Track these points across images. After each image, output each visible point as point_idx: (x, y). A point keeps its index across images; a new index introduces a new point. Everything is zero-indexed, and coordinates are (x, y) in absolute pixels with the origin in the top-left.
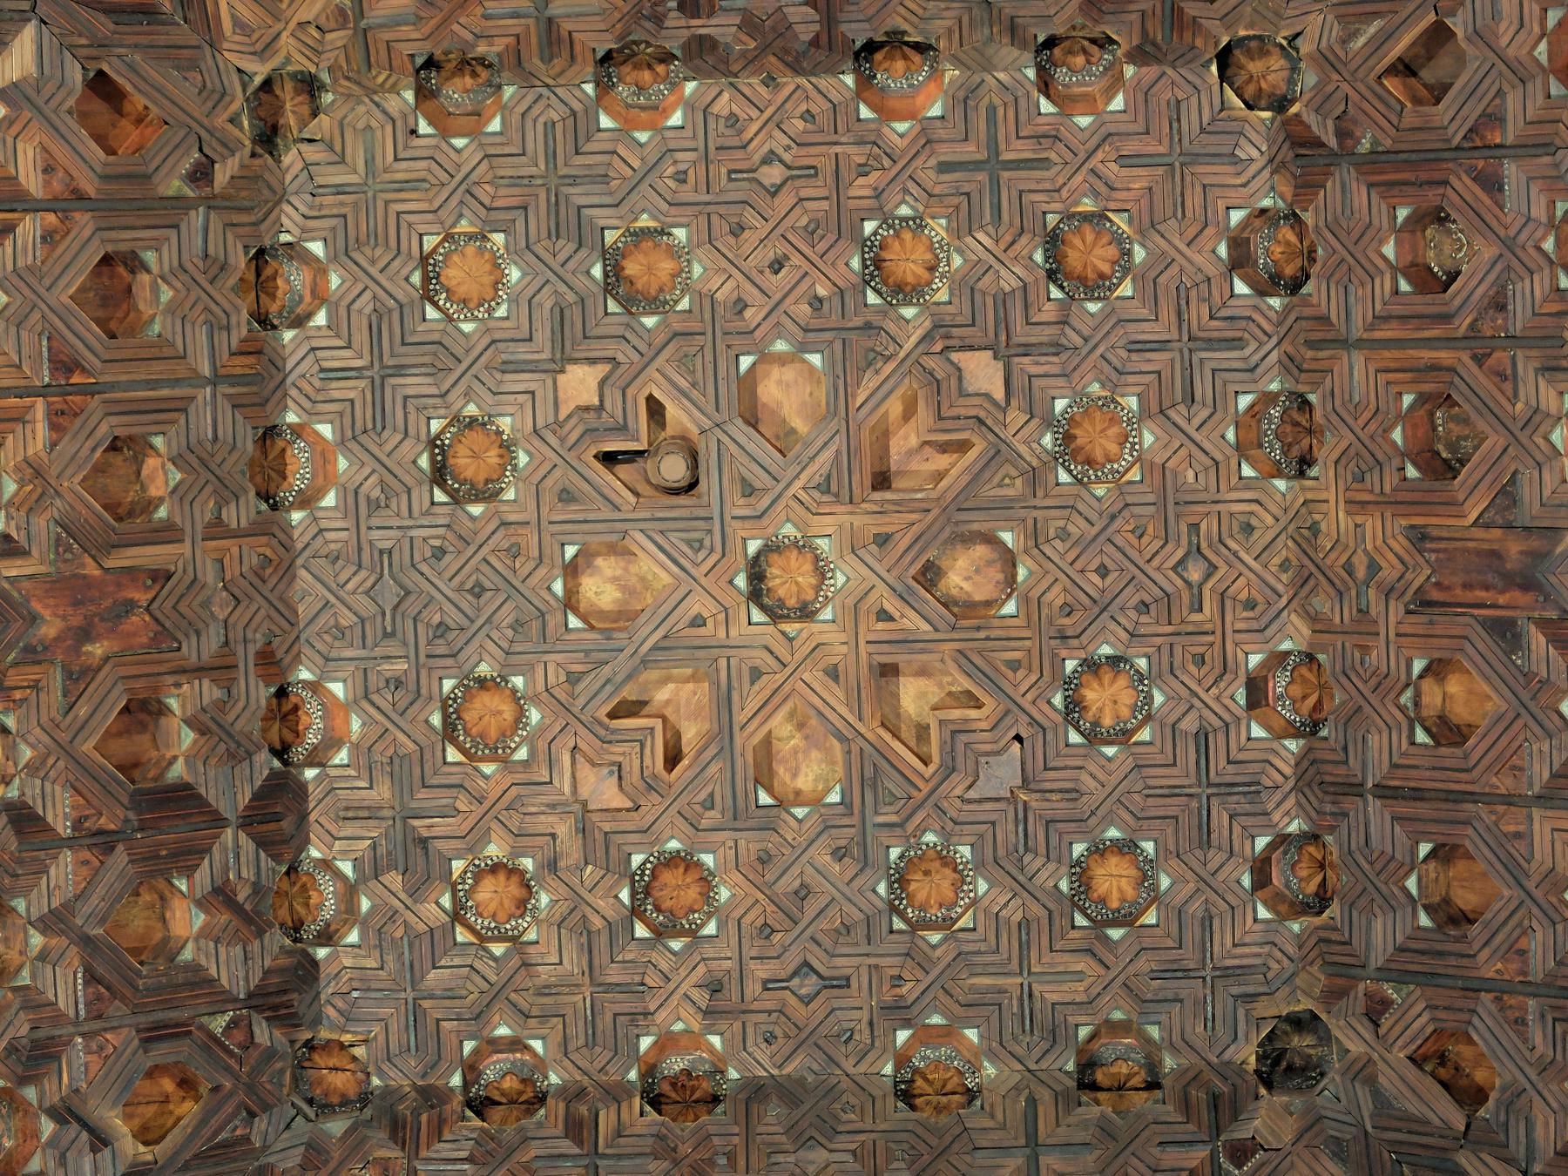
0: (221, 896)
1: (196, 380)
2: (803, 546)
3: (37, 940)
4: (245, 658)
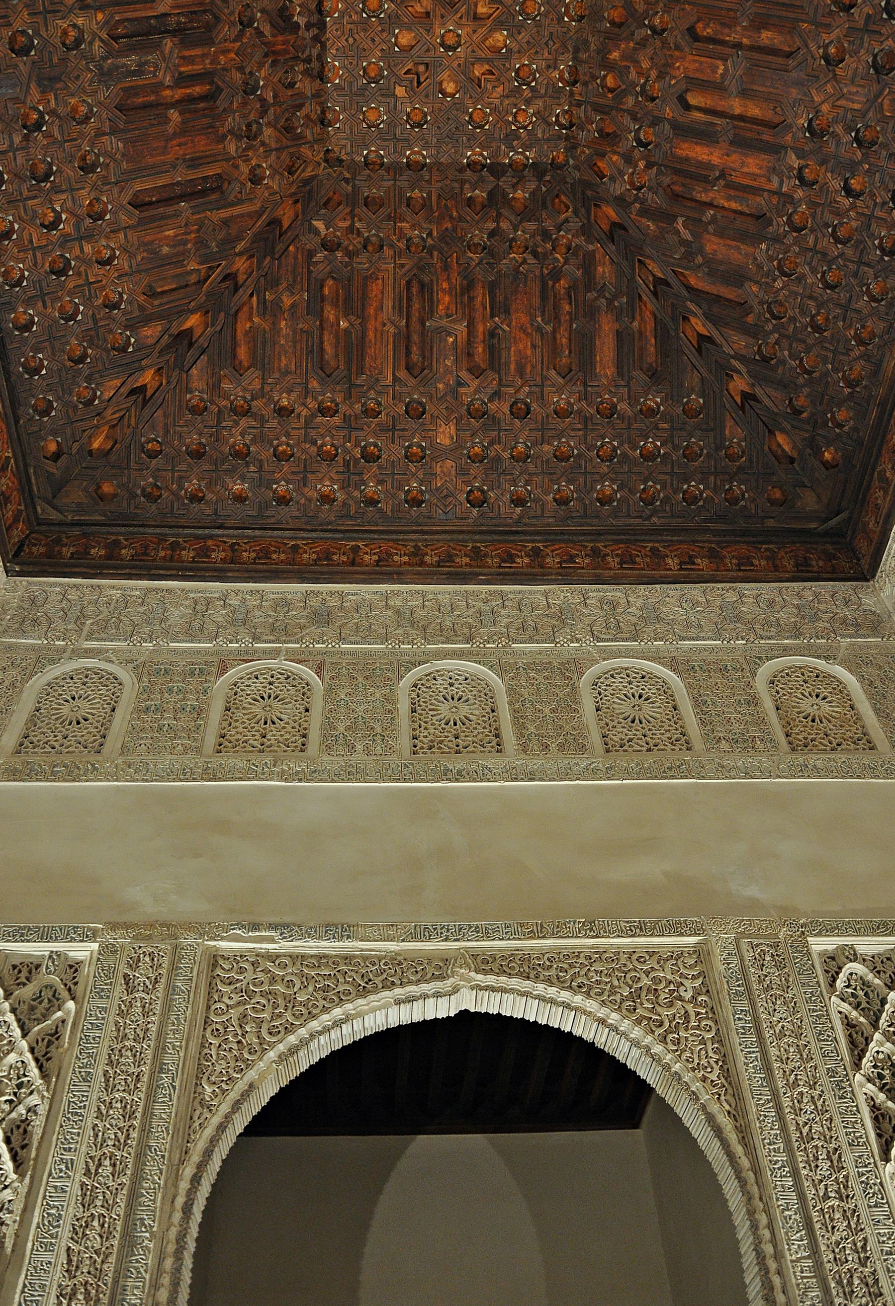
0: (514, 187)
1: (395, 184)
2: (443, 36)
3: (519, 233)
4: (460, 176)
